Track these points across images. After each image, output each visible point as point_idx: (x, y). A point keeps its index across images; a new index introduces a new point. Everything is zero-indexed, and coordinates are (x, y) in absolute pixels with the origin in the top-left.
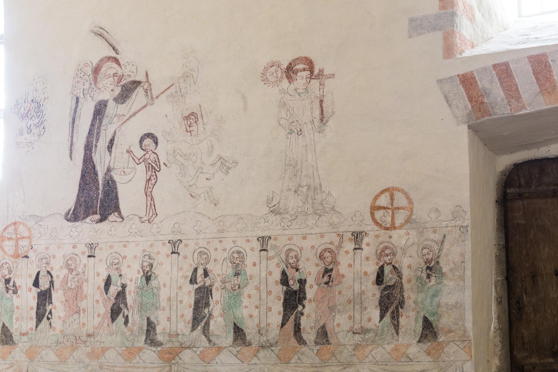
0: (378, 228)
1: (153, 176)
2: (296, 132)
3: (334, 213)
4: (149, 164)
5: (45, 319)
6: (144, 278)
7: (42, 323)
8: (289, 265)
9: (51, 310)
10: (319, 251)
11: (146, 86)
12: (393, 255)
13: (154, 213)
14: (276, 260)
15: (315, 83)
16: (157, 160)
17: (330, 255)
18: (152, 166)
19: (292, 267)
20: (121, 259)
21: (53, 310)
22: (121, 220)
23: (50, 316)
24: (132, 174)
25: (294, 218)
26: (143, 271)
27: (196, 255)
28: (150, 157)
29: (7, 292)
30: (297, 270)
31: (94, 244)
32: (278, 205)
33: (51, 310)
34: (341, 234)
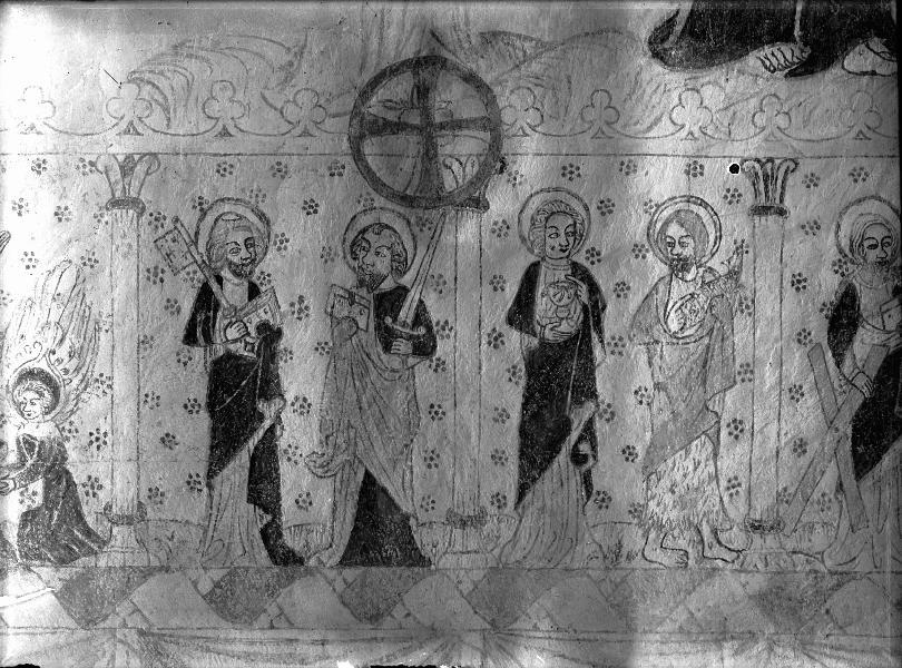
5: (563, 457)
7: (547, 474)
9: (591, 422)
21: (598, 424)
23: (584, 448)
29: (387, 348)
31: (777, 162)
33: (591, 422)
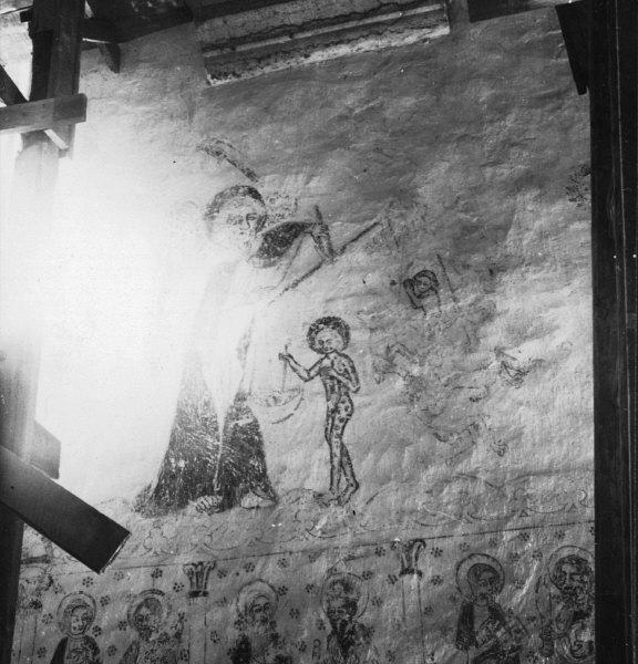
1: (343, 402)
4: (332, 378)
6: (334, 641)
11: (317, 231)
13: (352, 481)
16: (350, 369)
18: (339, 382)
20: (273, 595)
22: (270, 503)
24: (293, 404)
26: (333, 623)
27: (466, 567)
28: (332, 363)
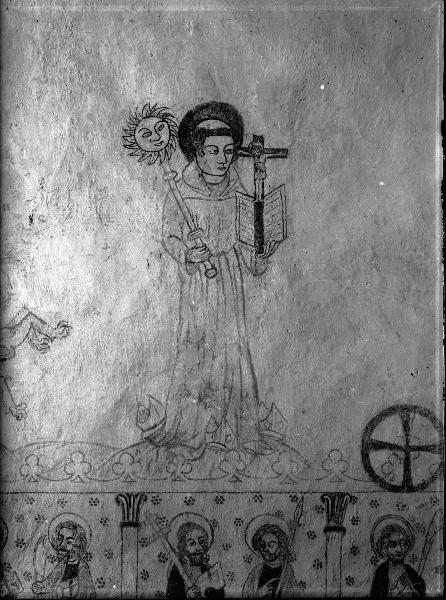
0: (378, 488)
2: (203, 270)
3: (284, 451)
8: (186, 557)
10: (254, 527)
12: (405, 544)
14: (155, 549)
15: (246, 165)
17: (277, 540)
19: (193, 563)
25: (196, 455)
30: (205, 569)
32: (160, 426)
34: (299, 495)
